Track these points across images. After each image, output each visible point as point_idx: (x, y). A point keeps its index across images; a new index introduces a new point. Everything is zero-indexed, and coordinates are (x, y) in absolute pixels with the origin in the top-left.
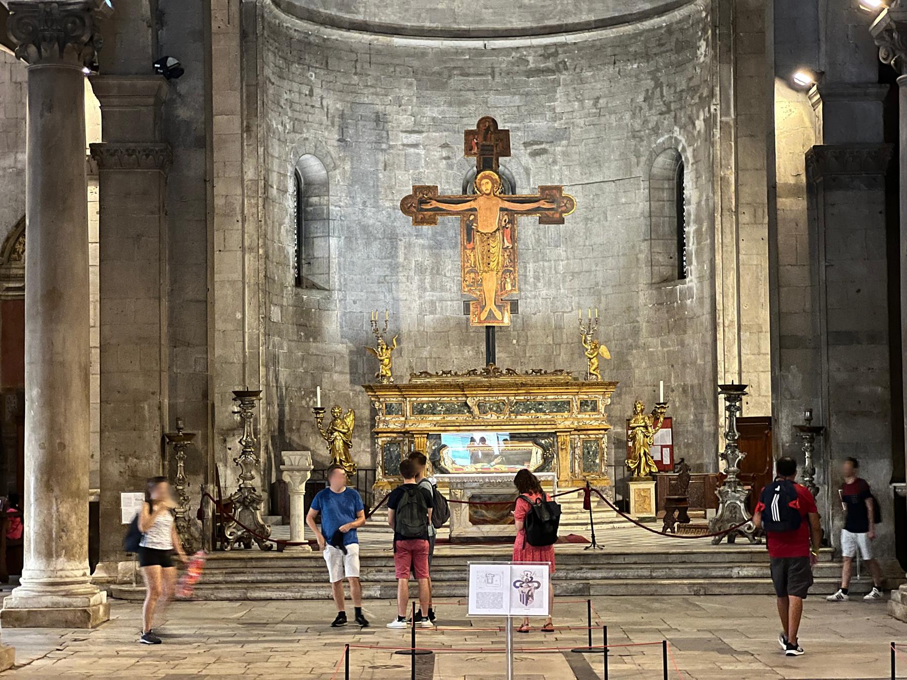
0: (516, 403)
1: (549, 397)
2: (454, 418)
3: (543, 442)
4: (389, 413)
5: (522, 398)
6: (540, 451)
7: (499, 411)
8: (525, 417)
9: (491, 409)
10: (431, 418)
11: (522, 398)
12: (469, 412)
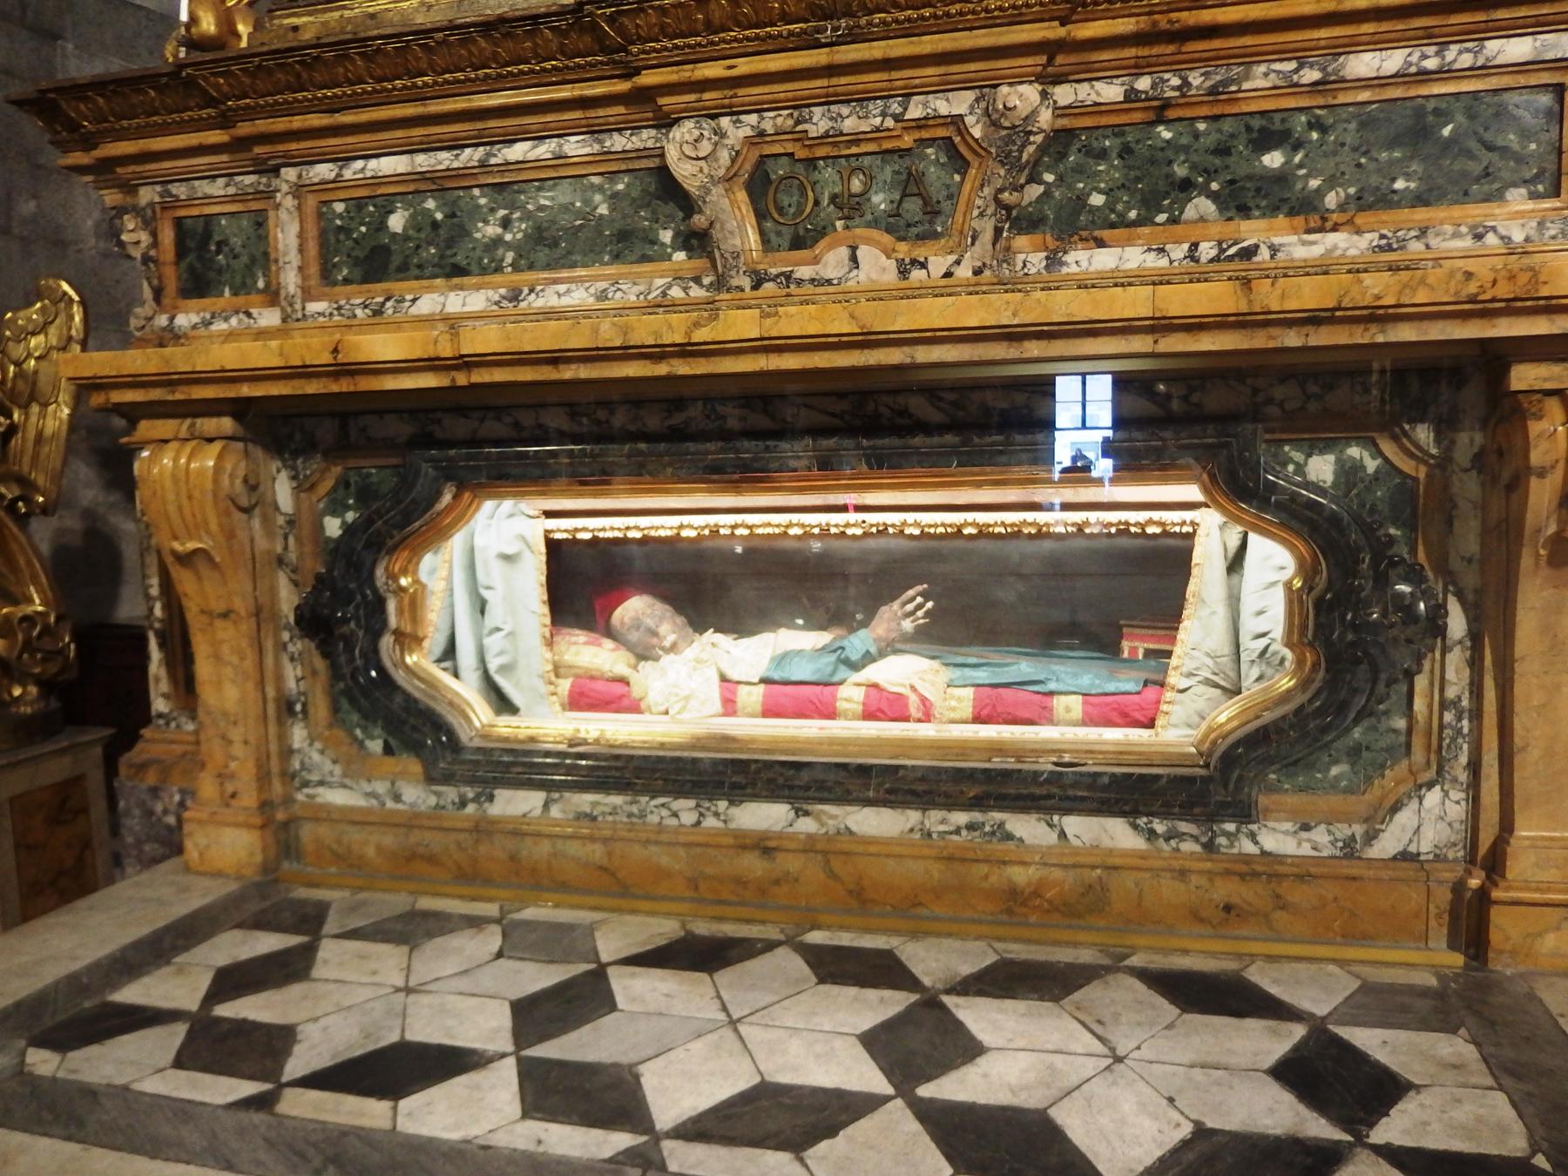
0: (1060, 140)
1: (1363, 64)
2: (579, 297)
3: (1322, 468)
4: (198, 285)
5: (1111, 92)
6: (1273, 562)
7: (918, 220)
8: (1134, 257)
9: (851, 207)
10: (428, 304)
11: (1111, 92)
12: (698, 241)
